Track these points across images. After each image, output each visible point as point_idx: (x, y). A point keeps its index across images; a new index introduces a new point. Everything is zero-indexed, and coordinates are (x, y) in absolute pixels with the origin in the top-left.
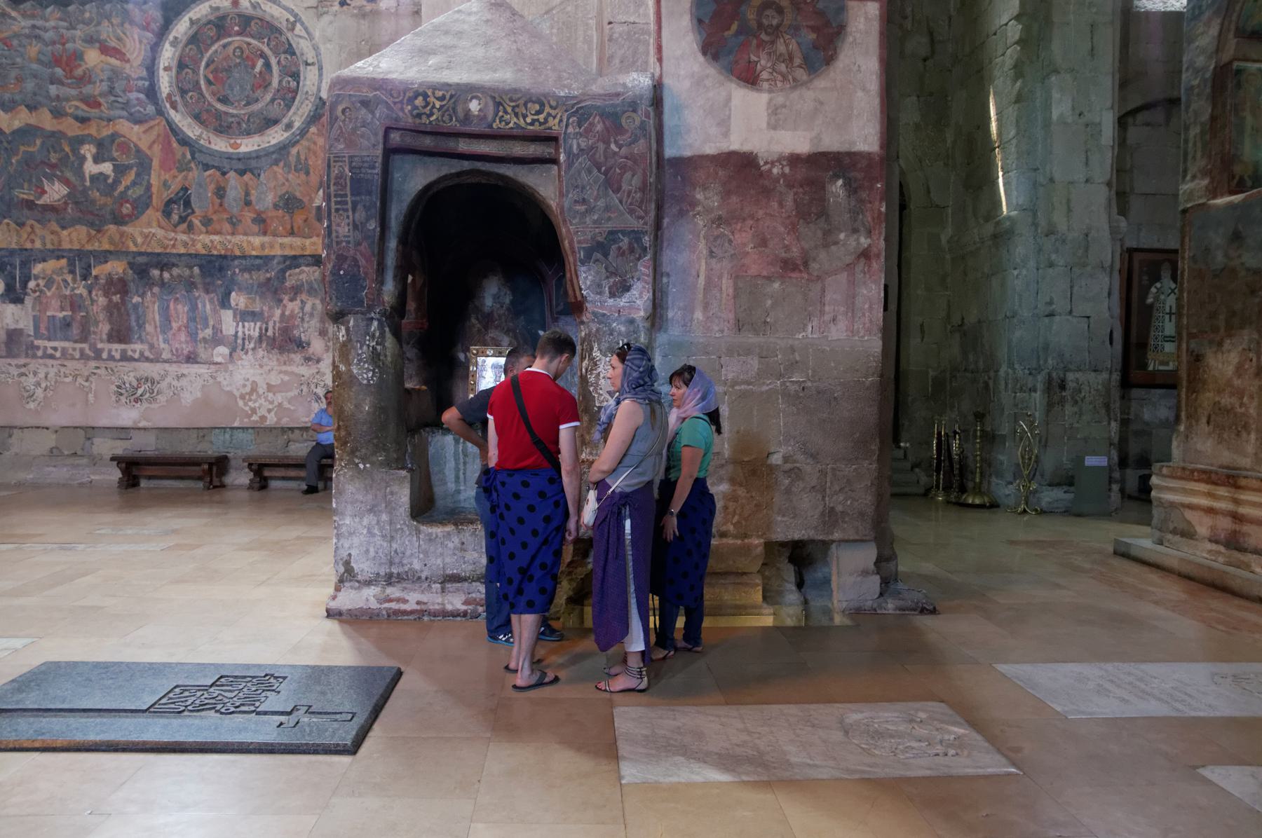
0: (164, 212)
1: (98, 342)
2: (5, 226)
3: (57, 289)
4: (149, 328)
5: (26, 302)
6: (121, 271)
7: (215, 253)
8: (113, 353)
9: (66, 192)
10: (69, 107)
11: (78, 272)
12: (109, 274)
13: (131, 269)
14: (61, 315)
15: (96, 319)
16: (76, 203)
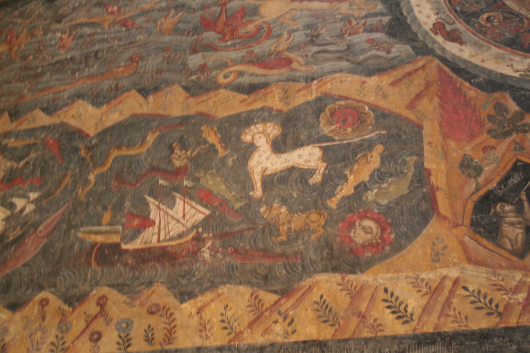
0: (475, 225)
9: (200, 217)
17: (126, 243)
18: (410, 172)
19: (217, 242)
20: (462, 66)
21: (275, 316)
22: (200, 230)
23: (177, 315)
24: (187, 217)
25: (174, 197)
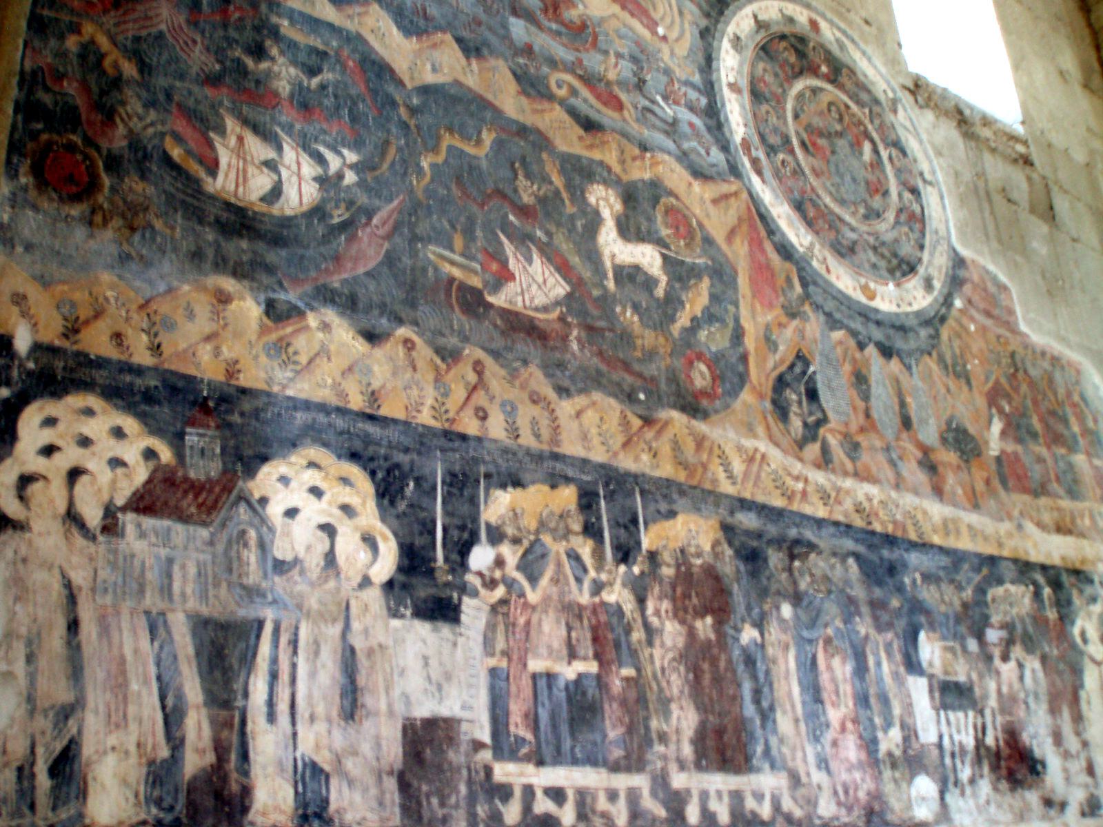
1: (673, 767)
2: (401, 351)
3: (555, 581)
4: (784, 723)
5: (463, 618)
6: (707, 548)
7: (877, 527)
8: (714, 805)
10: (559, 82)
11: (607, 535)
12: (682, 551)
13: (730, 544)
14: (569, 672)
15: (661, 690)
16: (590, 329)
17: (489, 294)
18: (731, 325)
19: (583, 334)
20: (763, 210)
21: (642, 445)
22: (564, 309)
23: (558, 413)
24: (548, 284)
25: (529, 250)
